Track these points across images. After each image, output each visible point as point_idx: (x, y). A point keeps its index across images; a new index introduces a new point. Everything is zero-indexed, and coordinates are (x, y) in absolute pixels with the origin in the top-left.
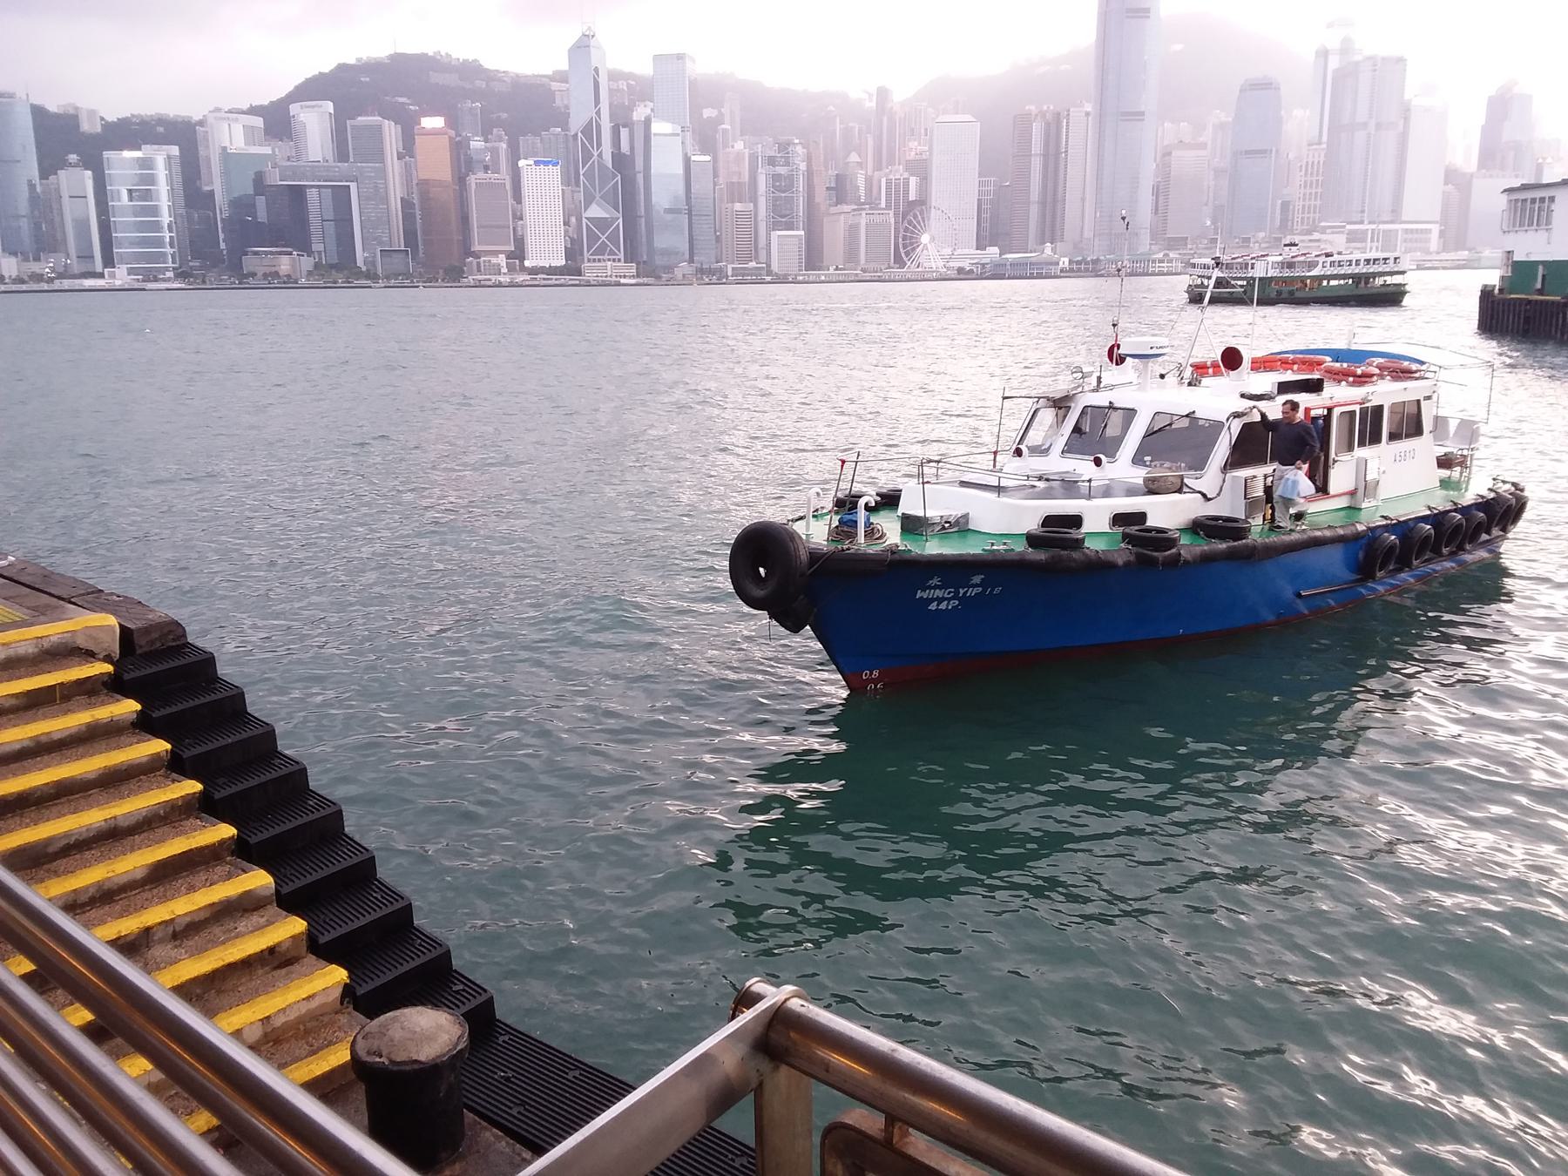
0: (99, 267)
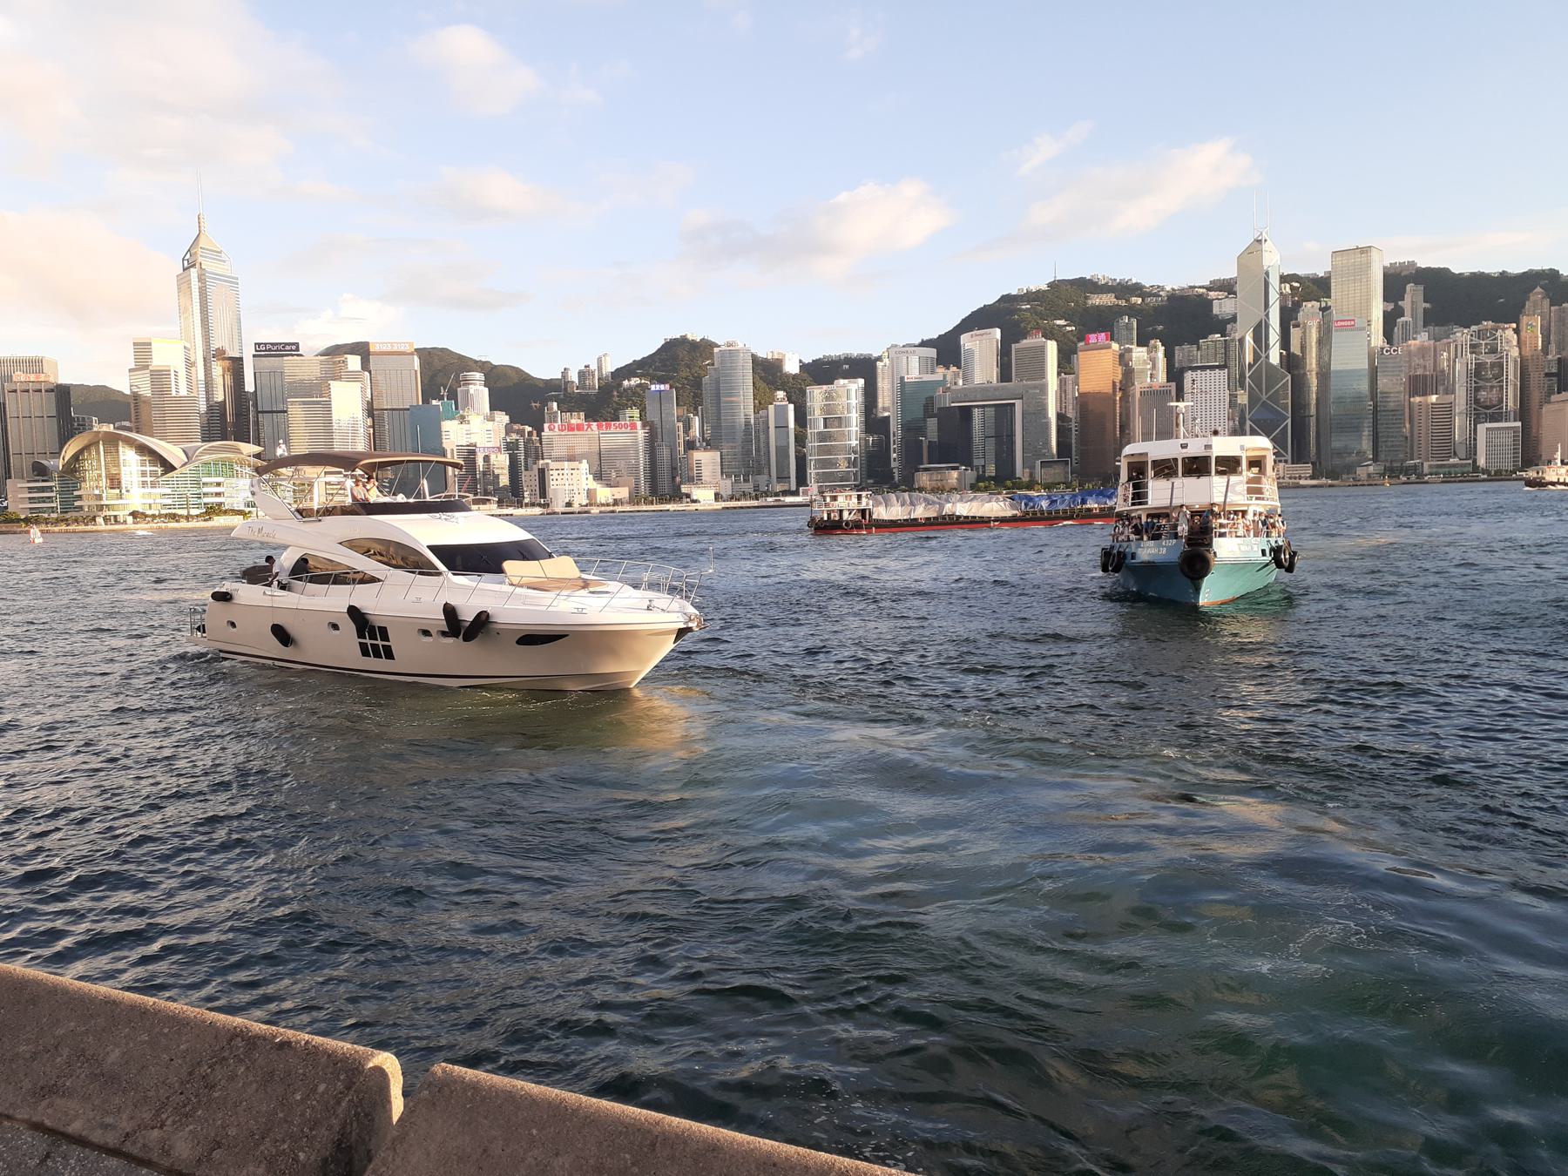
0: (793, 488)
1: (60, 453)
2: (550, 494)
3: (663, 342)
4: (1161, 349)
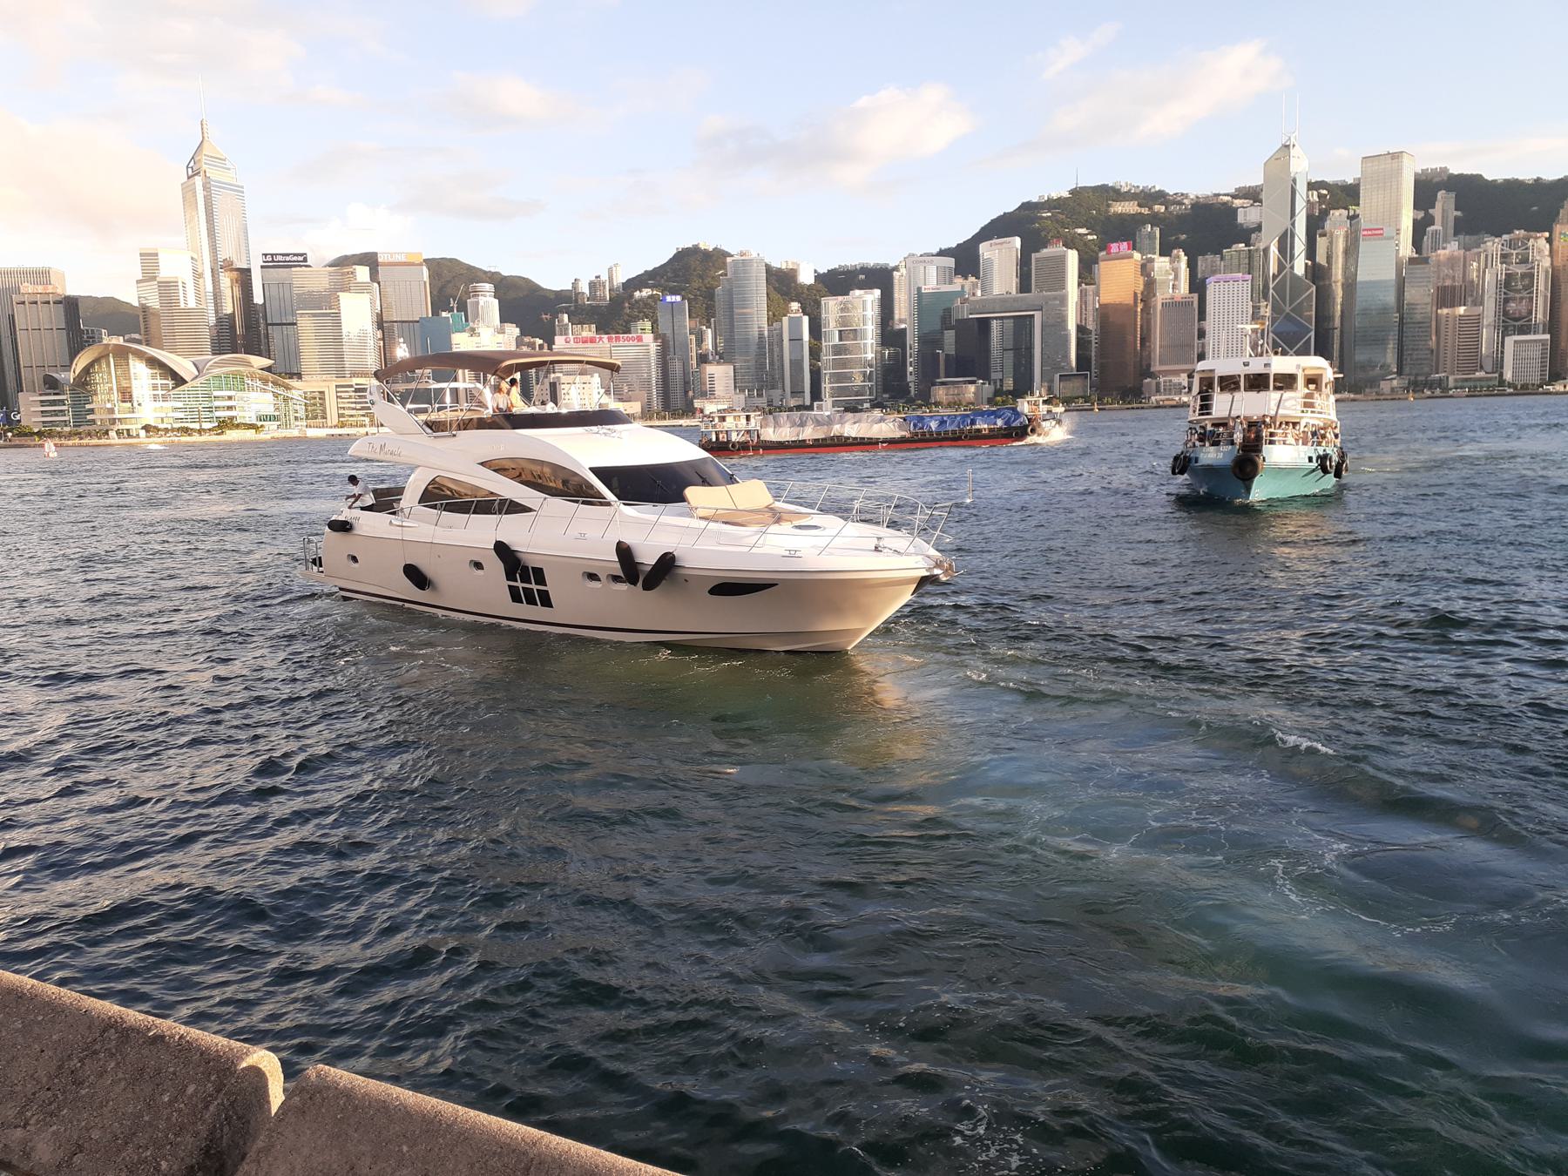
0: (808, 403)
1: (70, 366)
3: (675, 252)
4: (1184, 259)
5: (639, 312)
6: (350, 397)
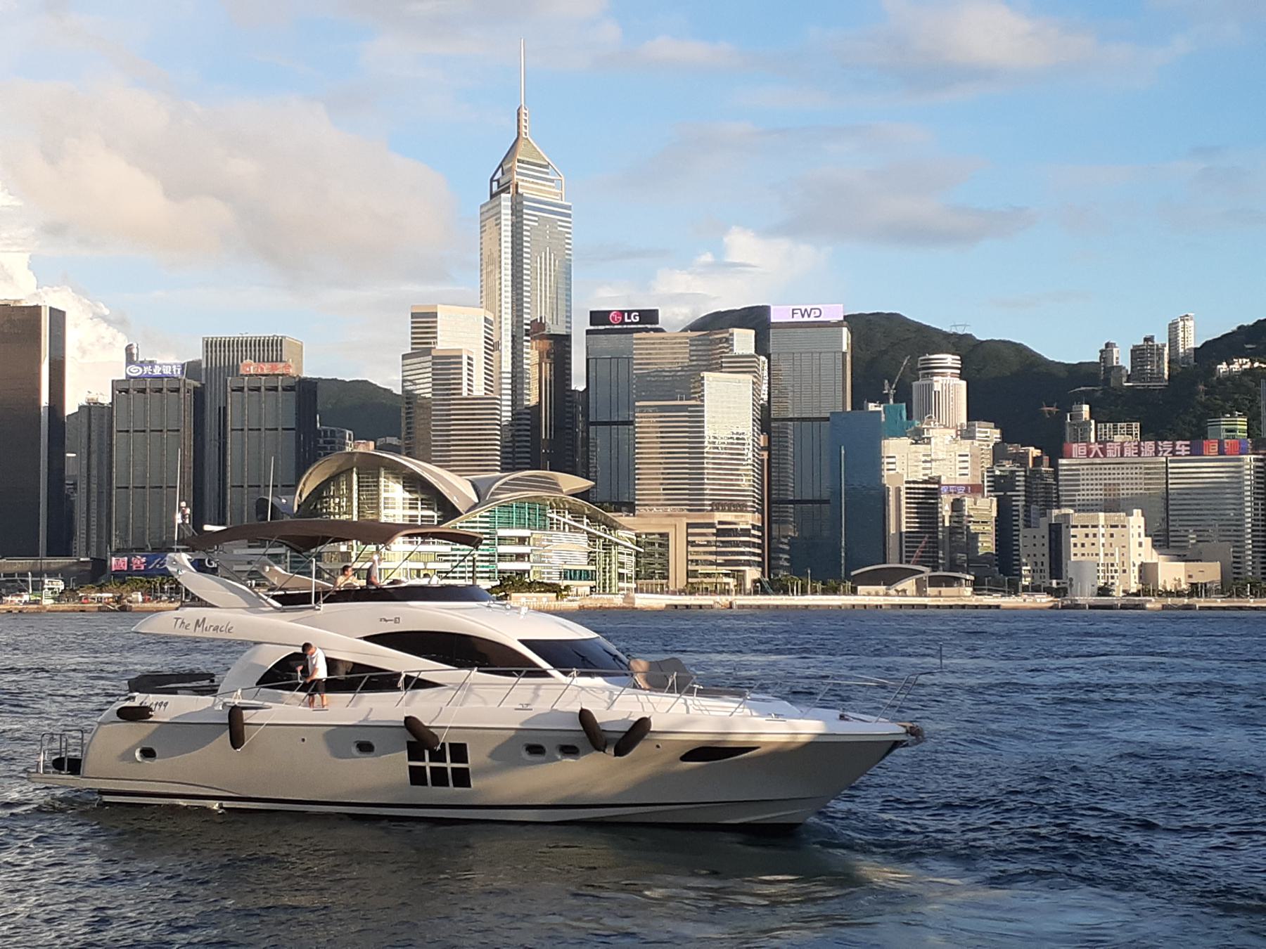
1: (296, 486)
2: (1070, 572)
5: (1227, 400)
6: (709, 544)
